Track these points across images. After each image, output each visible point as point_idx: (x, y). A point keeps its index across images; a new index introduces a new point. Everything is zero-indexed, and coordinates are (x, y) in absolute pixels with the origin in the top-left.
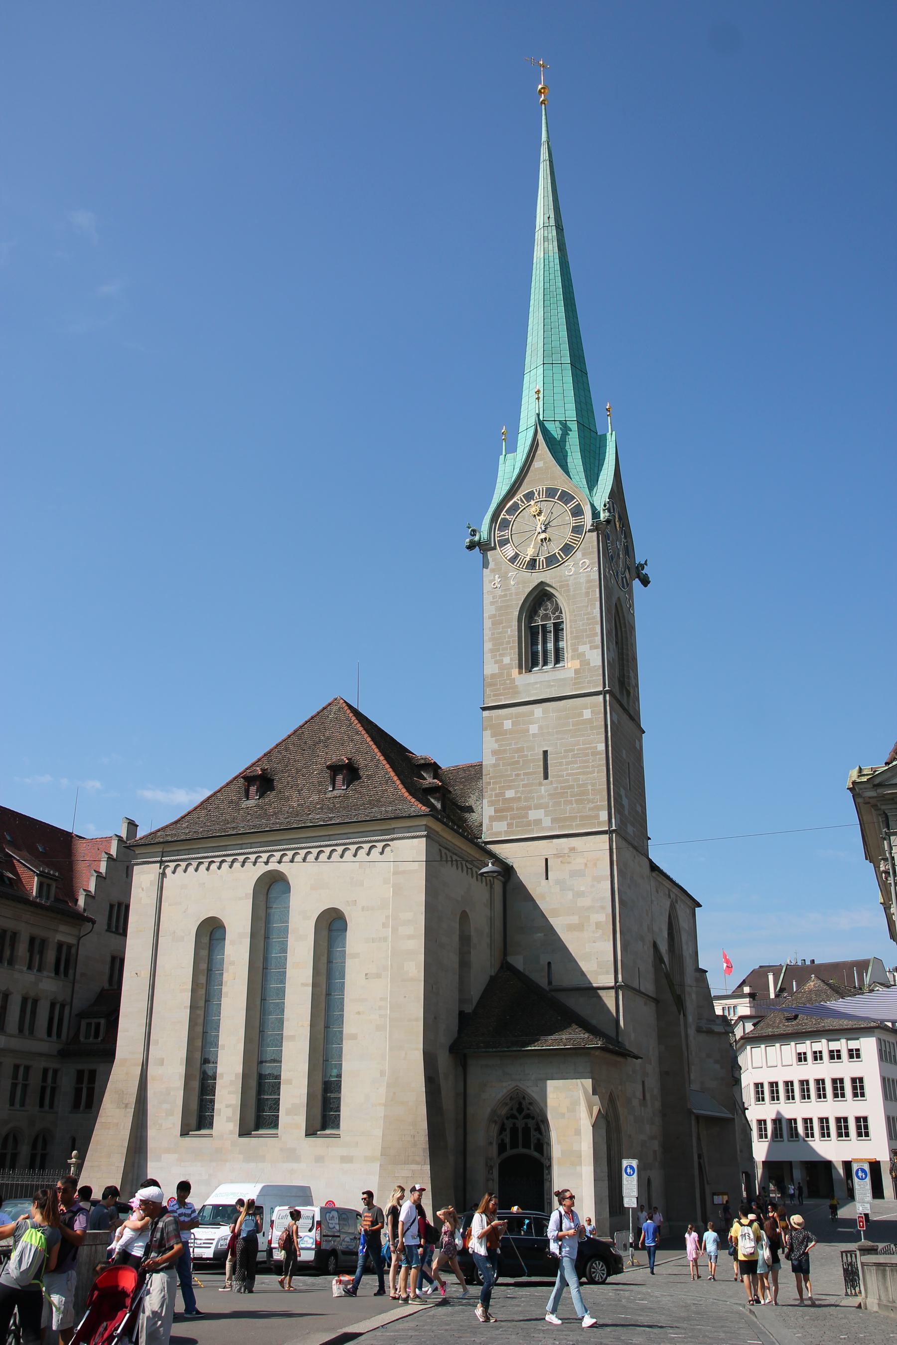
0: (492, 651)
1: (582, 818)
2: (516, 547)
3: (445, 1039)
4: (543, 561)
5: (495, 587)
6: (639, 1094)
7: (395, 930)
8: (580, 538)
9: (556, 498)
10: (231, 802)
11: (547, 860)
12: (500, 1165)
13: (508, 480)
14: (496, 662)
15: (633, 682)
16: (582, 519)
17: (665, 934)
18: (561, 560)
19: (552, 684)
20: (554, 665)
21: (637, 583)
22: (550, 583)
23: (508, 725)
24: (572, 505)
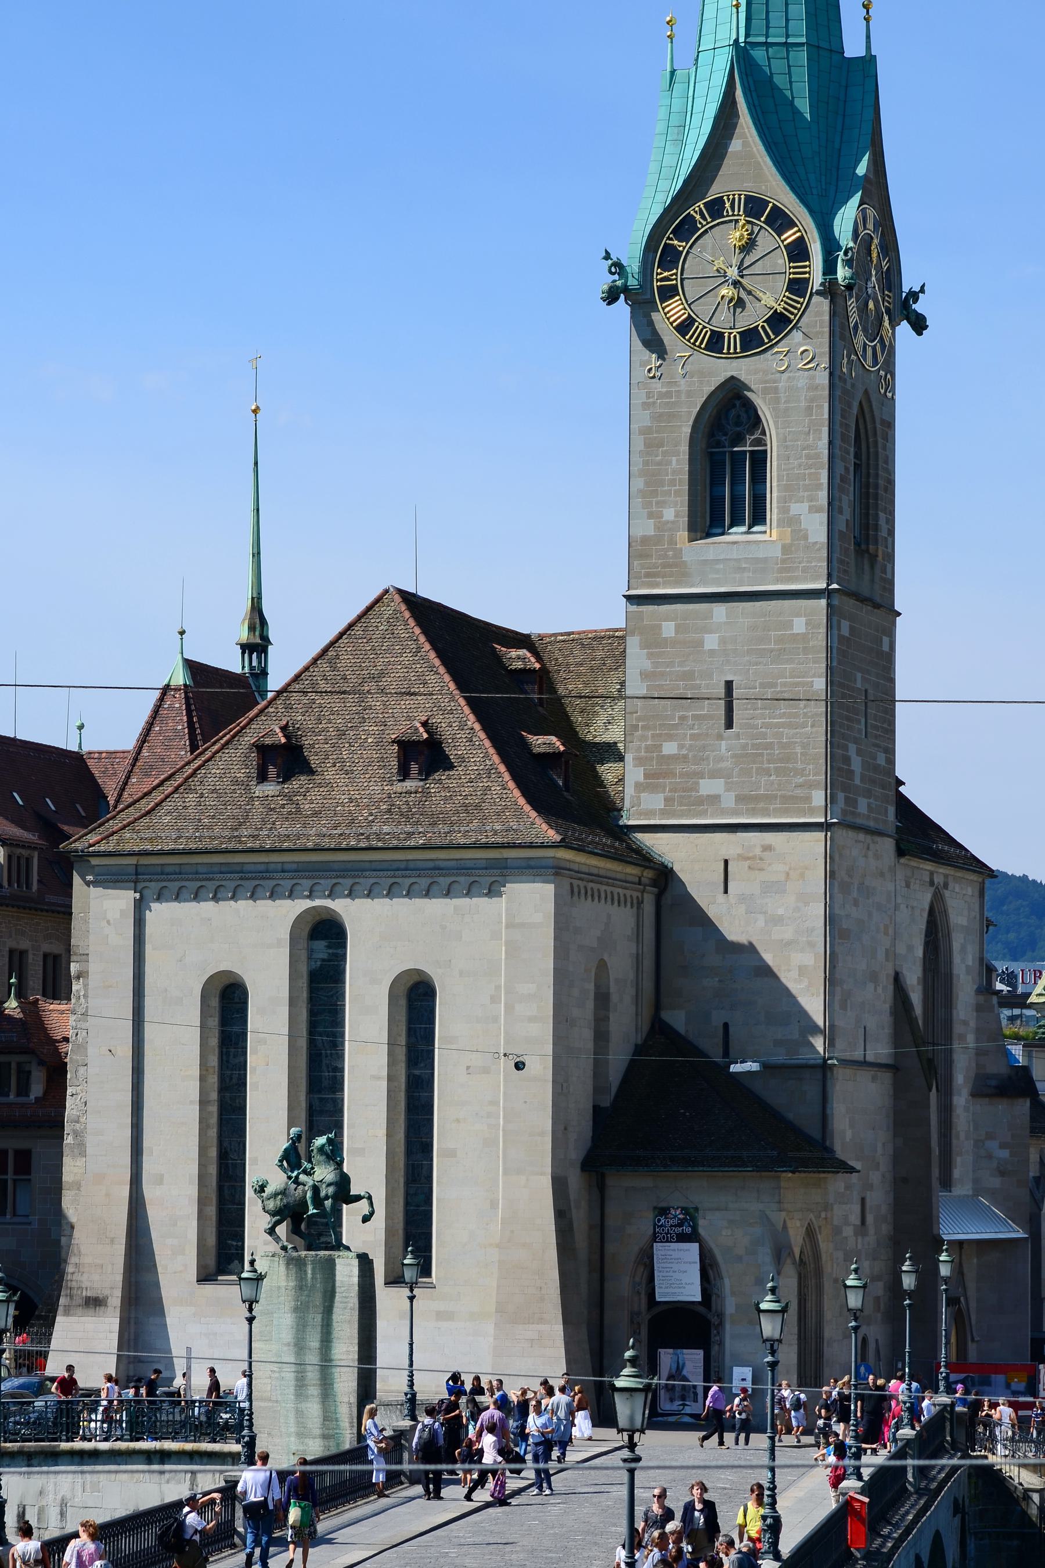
0: (643, 493)
1: (785, 799)
2: (689, 305)
3: (576, 1154)
4: (735, 336)
5: (651, 375)
6: (855, 1219)
7: (509, 1008)
8: (802, 304)
9: (762, 219)
10: (236, 782)
11: (726, 862)
12: (650, 1321)
13: (676, 130)
14: (651, 515)
15: (884, 533)
16: (805, 267)
17: (919, 952)
18: (766, 341)
19: (744, 566)
20: (750, 527)
21: (904, 328)
22: (746, 382)
23: (668, 629)
24: (790, 236)
